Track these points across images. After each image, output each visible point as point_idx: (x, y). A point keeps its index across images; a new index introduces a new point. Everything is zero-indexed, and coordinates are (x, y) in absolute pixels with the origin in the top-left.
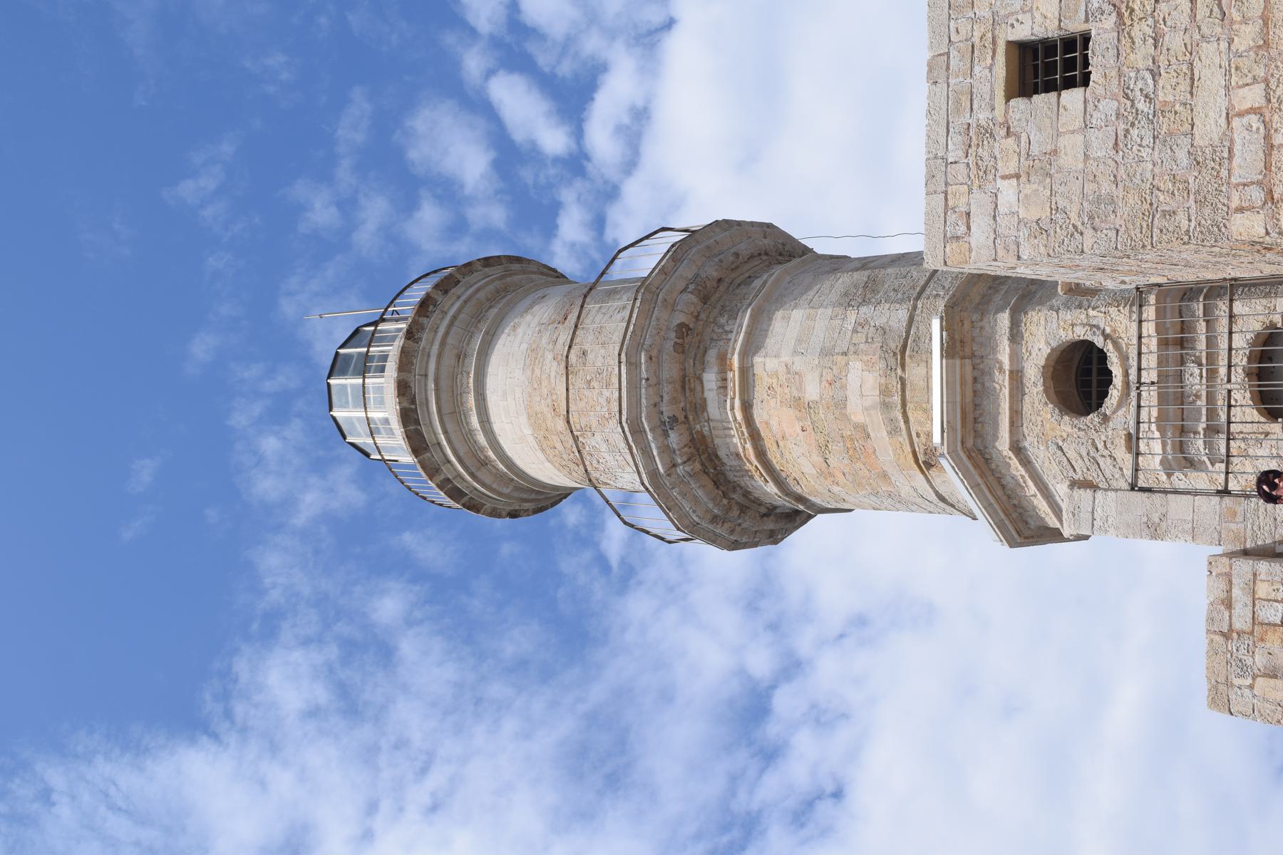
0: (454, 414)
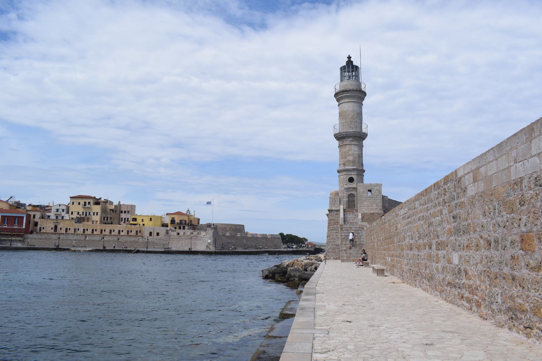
0: (347, 97)
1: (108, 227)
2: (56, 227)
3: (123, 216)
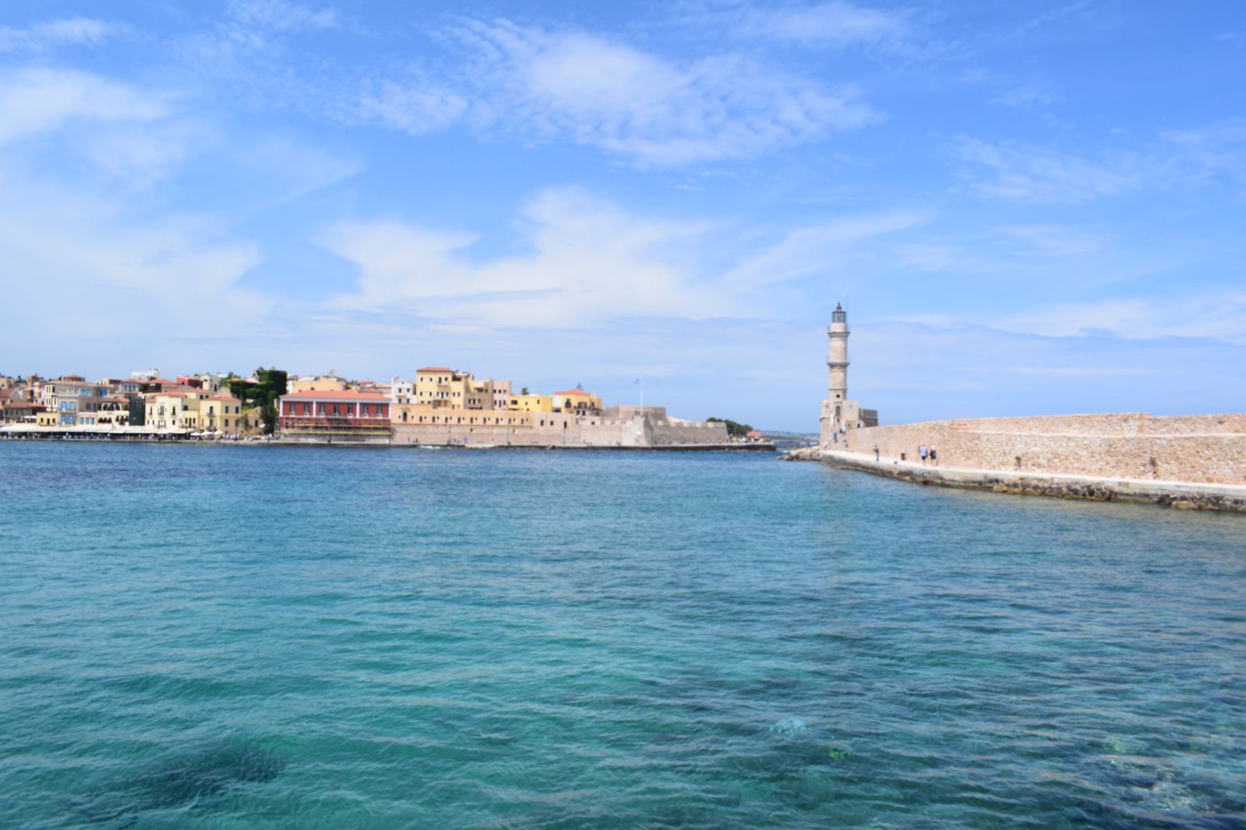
1: (479, 415)
2: (405, 415)
3: (497, 397)
